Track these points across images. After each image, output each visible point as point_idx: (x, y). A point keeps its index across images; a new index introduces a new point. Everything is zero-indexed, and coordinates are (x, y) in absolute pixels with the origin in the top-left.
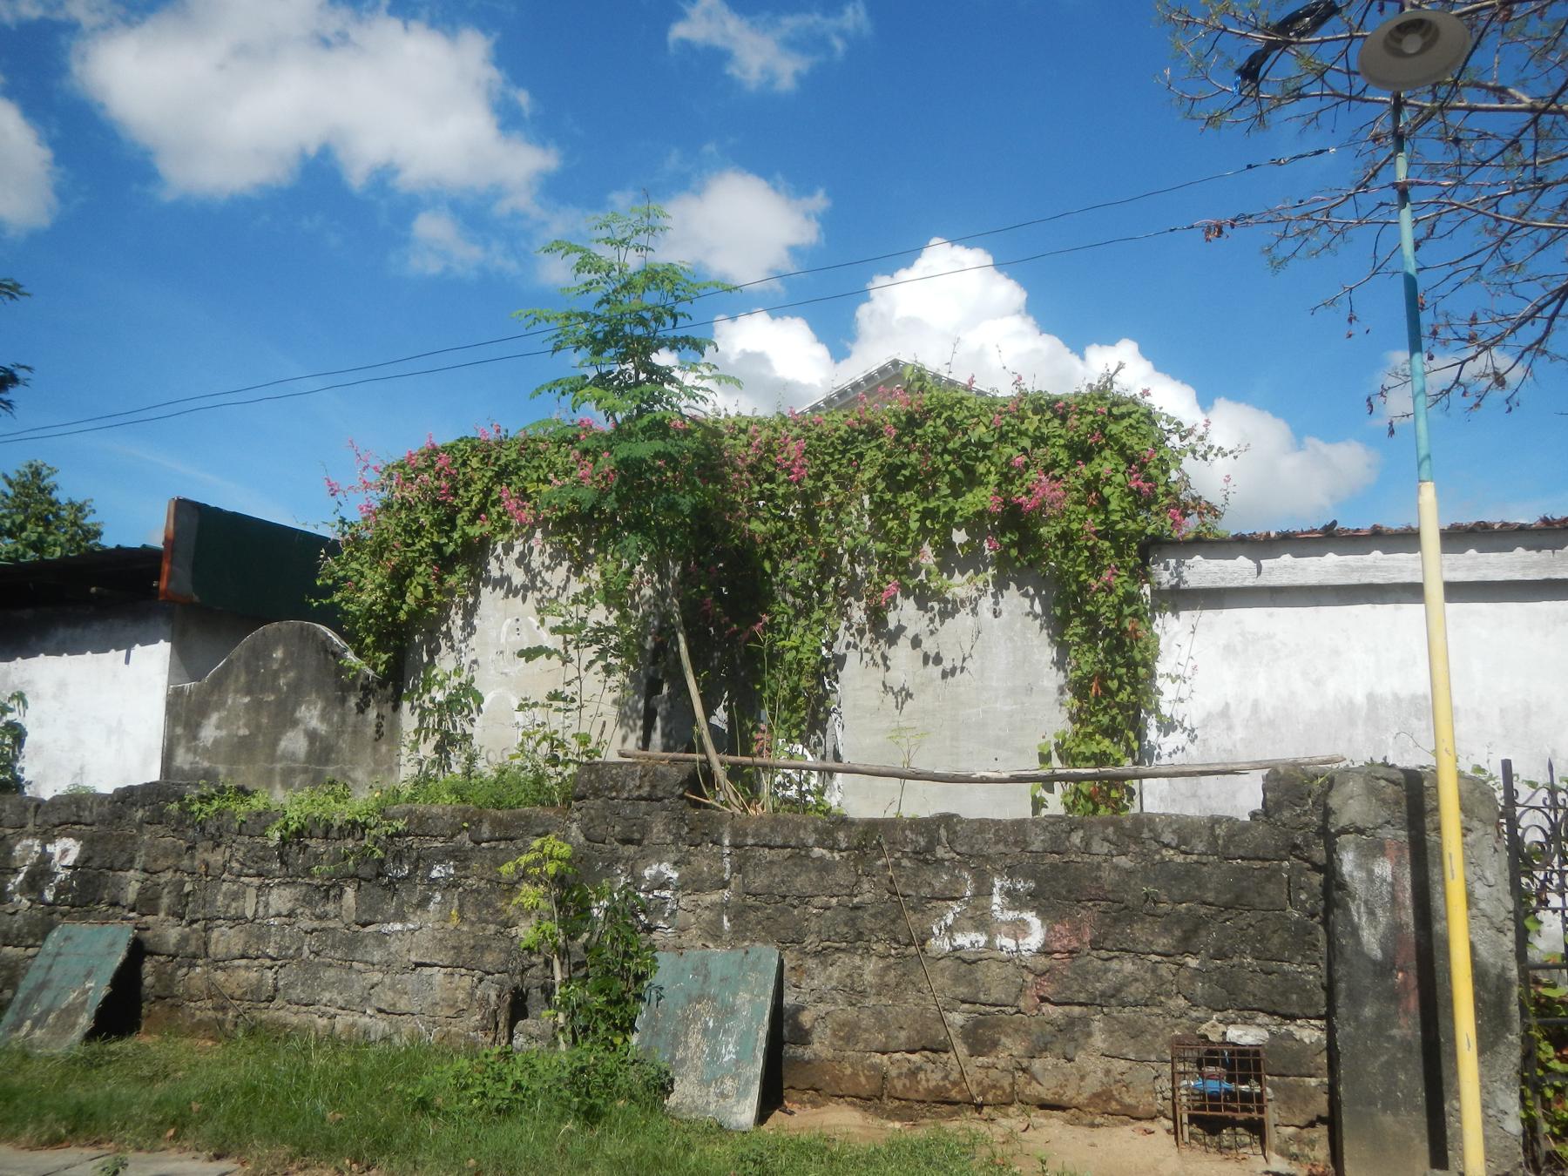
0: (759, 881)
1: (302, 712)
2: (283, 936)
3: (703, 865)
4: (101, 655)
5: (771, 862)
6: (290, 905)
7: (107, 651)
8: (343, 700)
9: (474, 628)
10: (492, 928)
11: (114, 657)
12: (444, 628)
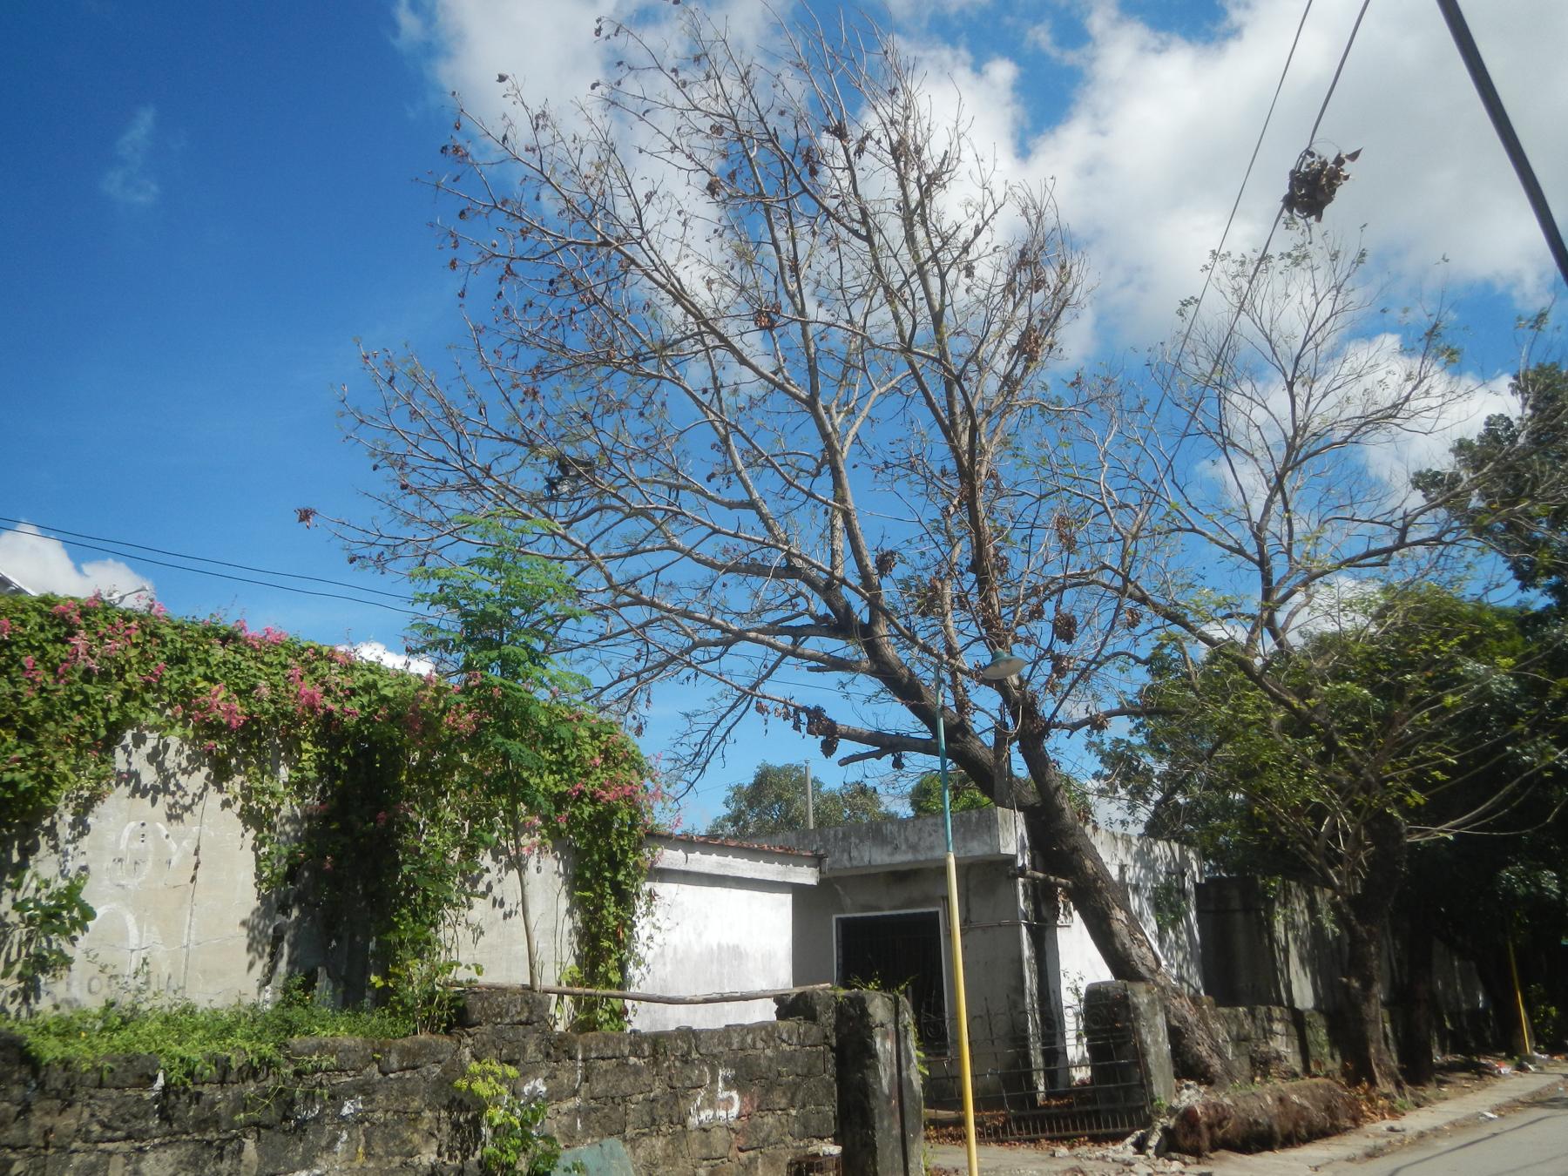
0: (599, 1088)
9: (87, 828)
10: (397, 1160)
12: (46, 823)
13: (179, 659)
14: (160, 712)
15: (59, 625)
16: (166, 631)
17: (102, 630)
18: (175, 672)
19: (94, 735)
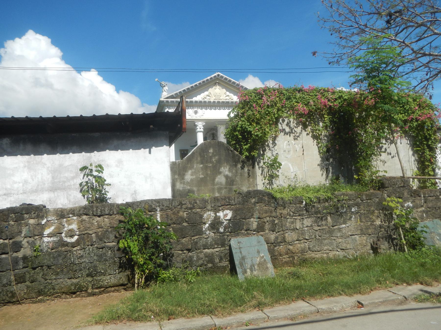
0: (430, 205)
1: (222, 169)
2: (310, 233)
3: (418, 202)
4: (137, 151)
5: (432, 200)
6: (311, 223)
7: (140, 149)
8: (236, 166)
9: (276, 144)
10: (369, 223)
11: (143, 152)
12: (267, 144)
13: (289, 98)
14: (287, 113)
15: (259, 95)
16: (284, 92)
17: (269, 95)
18: (288, 102)
19: (273, 121)
